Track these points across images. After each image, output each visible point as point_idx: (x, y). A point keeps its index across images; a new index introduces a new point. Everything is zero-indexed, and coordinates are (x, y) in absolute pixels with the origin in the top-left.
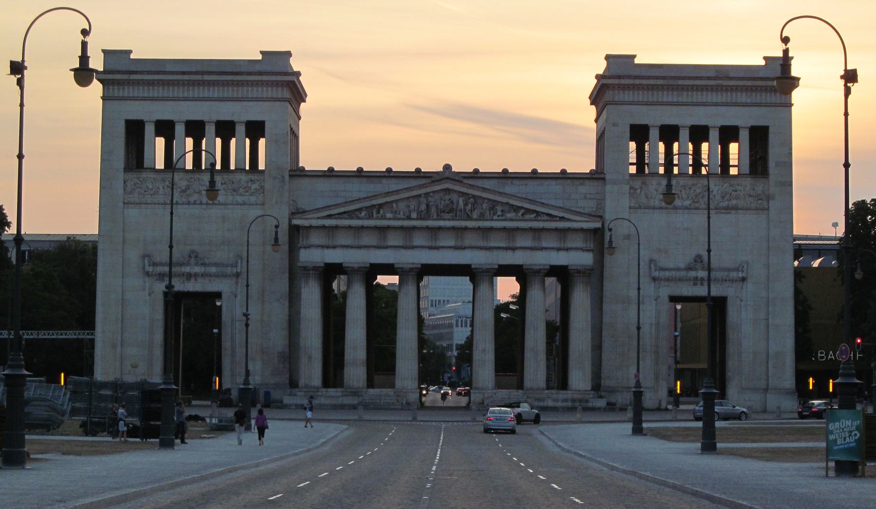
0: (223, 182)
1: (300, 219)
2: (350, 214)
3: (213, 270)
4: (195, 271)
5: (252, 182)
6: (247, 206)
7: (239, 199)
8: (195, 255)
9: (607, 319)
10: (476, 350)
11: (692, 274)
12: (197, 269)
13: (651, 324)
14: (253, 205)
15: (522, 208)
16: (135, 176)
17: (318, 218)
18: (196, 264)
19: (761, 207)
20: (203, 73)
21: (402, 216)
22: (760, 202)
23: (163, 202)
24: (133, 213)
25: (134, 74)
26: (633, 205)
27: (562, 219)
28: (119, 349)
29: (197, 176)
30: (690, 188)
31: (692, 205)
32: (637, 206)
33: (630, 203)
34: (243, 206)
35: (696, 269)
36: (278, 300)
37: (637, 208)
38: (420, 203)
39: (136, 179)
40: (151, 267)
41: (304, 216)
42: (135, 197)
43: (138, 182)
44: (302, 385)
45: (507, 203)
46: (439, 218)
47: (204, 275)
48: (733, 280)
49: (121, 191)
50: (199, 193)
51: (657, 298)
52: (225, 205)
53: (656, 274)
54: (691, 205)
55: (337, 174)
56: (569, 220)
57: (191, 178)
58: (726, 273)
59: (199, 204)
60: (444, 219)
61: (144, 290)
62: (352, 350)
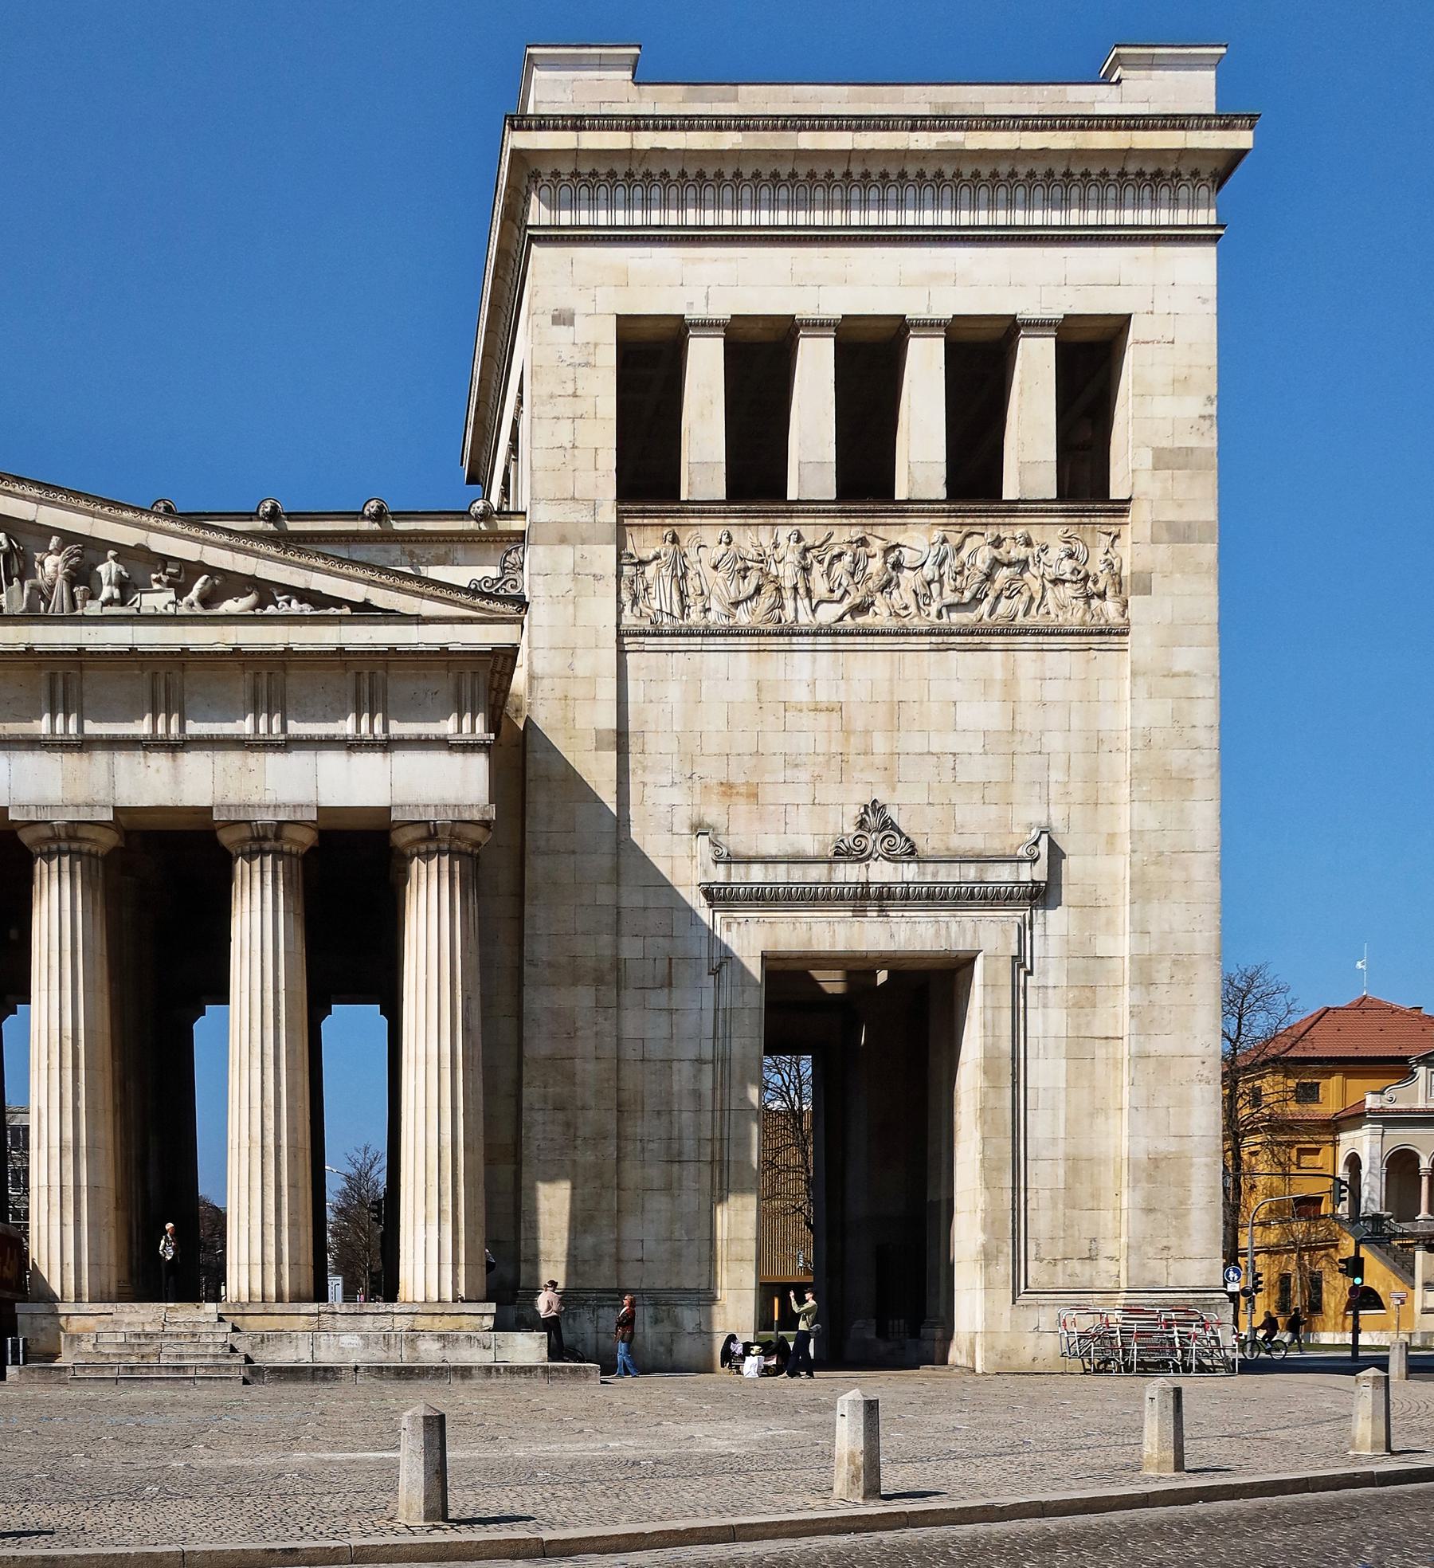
9: (538, 1046)
11: (849, 873)
13: (700, 1061)
19: (1102, 621)
22: (1095, 603)
26: (634, 621)
31: (847, 618)
32: (646, 624)
33: (619, 612)
35: (860, 857)
37: (645, 634)
48: (997, 896)
51: (721, 965)
53: (719, 874)
54: (841, 619)
58: (971, 872)
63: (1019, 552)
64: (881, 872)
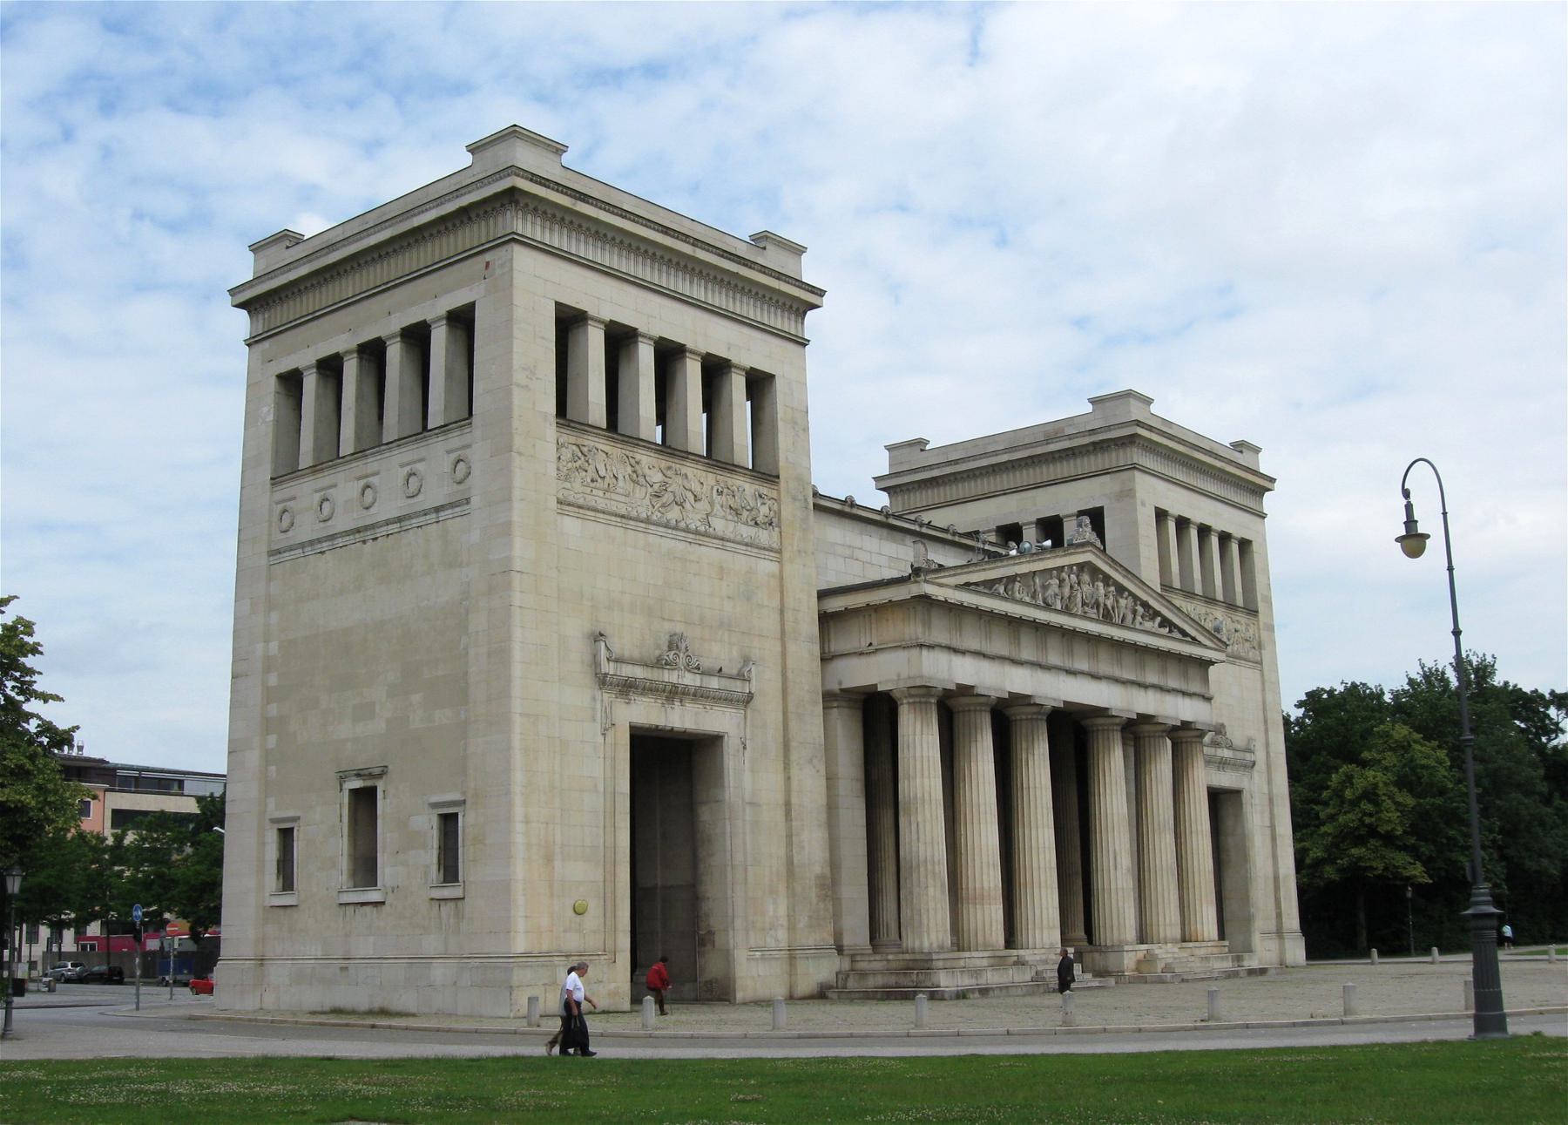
0: (720, 489)
1: (933, 583)
2: (989, 584)
3: (714, 683)
4: (686, 681)
5: (762, 501)
6: (756, 551)
7: (747, 532)
8: (683, 646)
10: (1116, 869)
12: (690, 680)
14: (764, 549)
15: (1157, 613)
16: (572, 439)
17: (957, 587)
18: (689, 668)
20: (696, 243)
21: (1042, 604)
23: (623, 512)
24: (571, 525)
25: (583, 201)
27: (1194, 641)
28: (557, 864)
29: (678, 466)
30: (1205, 619)
34: (749, 549)
36: (810, 761)
38: (1062, 581)
39: (574, 447)
40: (611, 664)
41: (936, 578)
42: (577, 489)
43: (580, 454)
44: (931, 944)
45: (1145, 605)
46: (1084, 617)
47: (699, 695)
49: (554, 473)
50: (681, 505)
52: (722, 539)
55: (860, 513)
56: (1200, 644)
57: (669, 468)
59: (683, 531)
60: (1092, 619)
61: (594, 720)
62: (991, 868)
63: (1239, 627)
64: (1226, 753)
